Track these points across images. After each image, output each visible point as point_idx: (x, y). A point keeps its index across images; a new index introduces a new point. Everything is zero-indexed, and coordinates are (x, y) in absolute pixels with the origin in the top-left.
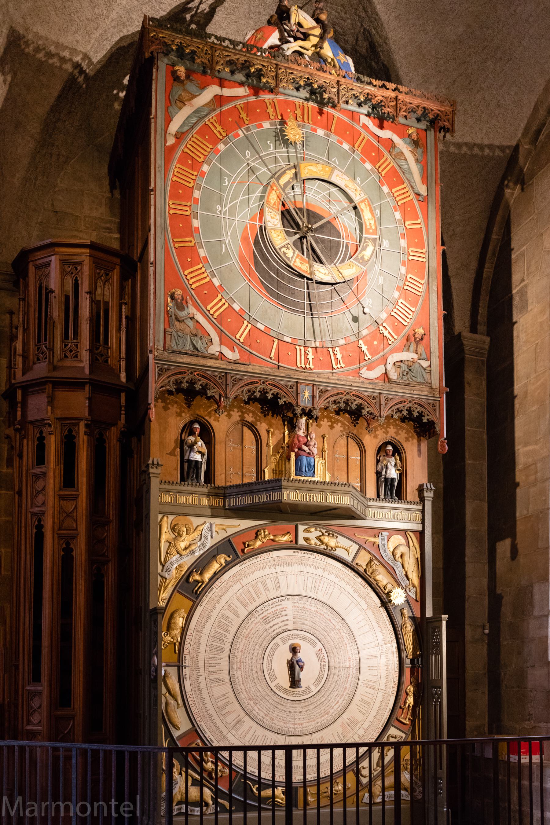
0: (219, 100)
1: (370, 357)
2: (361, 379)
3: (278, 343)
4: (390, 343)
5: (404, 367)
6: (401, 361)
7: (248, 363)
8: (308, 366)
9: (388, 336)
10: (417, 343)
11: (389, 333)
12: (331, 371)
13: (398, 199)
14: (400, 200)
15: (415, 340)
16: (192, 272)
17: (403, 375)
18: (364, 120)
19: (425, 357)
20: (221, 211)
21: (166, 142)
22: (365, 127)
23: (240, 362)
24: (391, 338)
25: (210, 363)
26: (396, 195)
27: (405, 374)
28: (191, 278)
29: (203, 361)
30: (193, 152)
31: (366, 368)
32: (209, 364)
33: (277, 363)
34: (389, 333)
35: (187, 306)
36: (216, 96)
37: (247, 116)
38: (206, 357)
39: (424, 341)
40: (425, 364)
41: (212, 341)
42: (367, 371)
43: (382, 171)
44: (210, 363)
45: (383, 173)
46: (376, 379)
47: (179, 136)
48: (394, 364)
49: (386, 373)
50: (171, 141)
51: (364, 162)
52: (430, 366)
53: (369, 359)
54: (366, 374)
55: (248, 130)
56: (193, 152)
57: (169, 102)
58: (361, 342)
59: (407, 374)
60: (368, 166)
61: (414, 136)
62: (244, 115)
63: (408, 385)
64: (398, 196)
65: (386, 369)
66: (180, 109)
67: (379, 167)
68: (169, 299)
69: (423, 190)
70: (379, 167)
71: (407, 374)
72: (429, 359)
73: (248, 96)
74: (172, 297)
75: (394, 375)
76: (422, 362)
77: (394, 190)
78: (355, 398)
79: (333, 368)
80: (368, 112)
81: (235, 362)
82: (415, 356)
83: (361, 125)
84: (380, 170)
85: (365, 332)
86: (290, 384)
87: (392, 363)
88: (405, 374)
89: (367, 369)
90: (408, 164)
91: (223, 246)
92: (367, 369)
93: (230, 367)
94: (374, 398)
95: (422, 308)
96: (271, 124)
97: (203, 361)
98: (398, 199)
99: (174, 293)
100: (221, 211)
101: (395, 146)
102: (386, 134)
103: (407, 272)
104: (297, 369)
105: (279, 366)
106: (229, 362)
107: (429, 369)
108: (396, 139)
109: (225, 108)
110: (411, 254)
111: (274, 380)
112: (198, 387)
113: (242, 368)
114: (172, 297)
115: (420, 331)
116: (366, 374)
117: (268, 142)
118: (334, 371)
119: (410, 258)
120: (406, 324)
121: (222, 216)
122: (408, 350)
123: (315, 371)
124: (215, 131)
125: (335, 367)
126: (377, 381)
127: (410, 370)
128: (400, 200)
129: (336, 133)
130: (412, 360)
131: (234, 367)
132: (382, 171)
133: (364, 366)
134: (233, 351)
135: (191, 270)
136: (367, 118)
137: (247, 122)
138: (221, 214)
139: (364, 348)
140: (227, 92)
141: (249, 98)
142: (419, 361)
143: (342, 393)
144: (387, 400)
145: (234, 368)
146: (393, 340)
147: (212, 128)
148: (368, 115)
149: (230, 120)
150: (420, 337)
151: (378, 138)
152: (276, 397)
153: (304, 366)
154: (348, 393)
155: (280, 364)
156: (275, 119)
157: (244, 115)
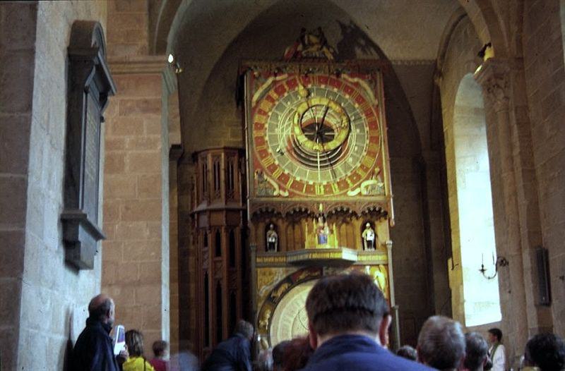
0: (274, 82)
5: (370, 188)
22: (344, 79)
25: (274, 199)
29: (271, 199)
40: (381, 185)
44: (274, 199)
47: (258, 102)
50: (254, 105)
54: (351, 193)
57: (251, 90)
62: (286, 87)
69: (376, 102)
72: (383, 181)
75: (364, 192)
76: (379, 184)
82: (376, 182)
97: (271, 199)
102: (356, 80)
112: (270, 210)
113: (290, 199)
115: (377, 170)
116: (351, 193)
139: (349, 181)
140: (278, 78)
151: (352, 83)
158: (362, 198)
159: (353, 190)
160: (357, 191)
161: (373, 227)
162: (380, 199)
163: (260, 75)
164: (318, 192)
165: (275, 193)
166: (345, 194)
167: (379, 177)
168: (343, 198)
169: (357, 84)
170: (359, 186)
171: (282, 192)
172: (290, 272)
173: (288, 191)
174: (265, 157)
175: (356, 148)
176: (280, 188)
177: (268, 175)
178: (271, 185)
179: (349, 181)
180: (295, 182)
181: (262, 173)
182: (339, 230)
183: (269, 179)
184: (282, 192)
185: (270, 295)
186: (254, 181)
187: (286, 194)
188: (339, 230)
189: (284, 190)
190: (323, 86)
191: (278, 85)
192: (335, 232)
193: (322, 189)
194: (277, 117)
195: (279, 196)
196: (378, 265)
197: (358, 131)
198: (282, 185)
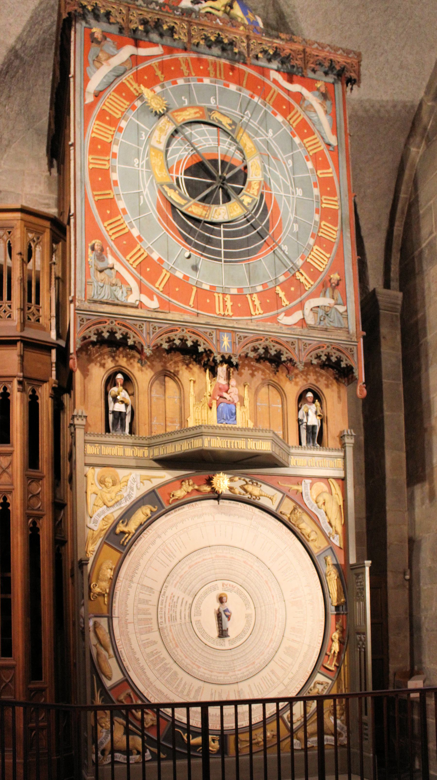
1: (287, 303)
2: (280, 325)
3: (197, 291)
4: (307, 289)
5: (321, 312)
6: (318, 307)
7: (168, 311)
8: (226, 313)
9: (305, 282)
10: (334, 288)
11: (305, 279)
12: (249, 318)
13: (309, 149)
14: (311, 150)
15: (331, 285)
16: (111, 224)
17: (321, 320)
18: (274, 75)
19: (342, 302)
20: (138, 165)
21: (85, 100)
22: (275, 82)
23: (159, 310)
24: (307, 284)
26: (307, 145)
27: (322, 319)
28: (111, 229)
30: (110, 109)
31: (283, 314)
32: (129, 313)
33: (196, 310)
34: (305, 279)
35: (107, 257)
36: (132, 56)
37: (162, 73)
38: (126, 306)
39: (340, 287)
40: (341, 309)
41: (131, 291)
42: (285, 318)
43: (294, 122)
45: (294, 125)
46: (295, 324)
47: (98, 95)
48: (311, 310)
49: (304, 319)
51: (276, 114)
52: (346, 311)
53: (286, 305)
55: (163, 86)
56: (110, 109)
57: (86, 64)
58: (278, 288)
59: (324, 319)
60: (280, 118)
61: (323, 89)
62: (159, 73)
63: (326, 330)
64: (309, 146)
65: (303, 315)
66: (98, 68)
67: (290, 119)
68: (90, 250)
69: (333, 140)
70: (290, 119)
71: (324, 319)
73: (162, 55)
74: (93, 249)
75: (310, 320)
76: (338, 307)
77: (305, 141)
78: (274, 344)
79: (252, 315)
80: (278, 67)
81: (155, 311)
82: (332, 302)
83: (272, 80)
84: (291, 122)
85: (282, 279)
86: (209, 331)
87: (309, 309)
88: (322, 319)
89: (285, 315)
90: (317, 116)
91: (141, 197)
92: (285, 315)
93: (150, 316)
94: (293, 344)
95: (337, 254)
96: (185, 81)
98: (309, 149)
99: (94, 245)
100: (138, 165)
101: (305, 99)
102: (295, 88)
103: (321, 219)
104: (216, 316)
105: (198, 313)
106: (149, 310)
107: (345, 313)
108: (305, 92)
109: (141, 67)
110: (324, 201)
111: (193, 327)
112: (118, 336)
113: (161, 316)
114: (93, 249)
115: (335, 277)
117: (183, 98)
118: (253, 317)
119: (324, 206)
120: (321, 270)
121: (140, 168)
122: (324, 295)
123: (234, 318)
124: (132, 89)
125: (253, 313)
126: (295, 327)
127: (327, 315)
128: (311, 150)
129: (248, 87)
130: (328, 305)
131: (154, 315)
132: (294, 122)
133: (282, 312)
134: (152, 299)
135: (110, 221)
136: (277, 73)
137: (162, 79)
138: (139, 167)
139: (282, 294)
140: (142, 52)
141: (164, 56)
142: (336, 306)
143: (261, 340)
144: (305, 345)
145: (154, 316)
146: (310, 286)
147: (129, 86)
148: (278, 70)
149: (146, 77)
150: (336, 282)
151: (288, 92)
152: (196, 344)
153: (223, 313)
154: (267, 340)
155: (199, 312)
156: (189, 75)
157: (159, 73)
158: (305, 331)
159: (288, 313)
160: (297, 316)
161: (317, 397)
162: (343, 336)
163: (105, 38)
164: (219, 310)
165: (132, 299)
166: (274, 319)
167: (337, 294)
168: (269, 326)
169: (299, 97)
170: (301, 306)
171: (145, 299)
172: (156, 482)
173: (158, 297)
174: (110, 217)
175: (296, 228)
176: (142, 289)
177: (114, 255)
178: (124, 281)
179: (282, 294)
180: (173, 278)
181: (102, 250)
182: (256, 401)
183: (118, 267)
184: (145, 299)
185: (115, 527)
186: (87, 263)
187: (154, 304)
188: (256, 401)
189: (150, 295)
190: (233, 87)
191: (141, 67)
192: (246, 403)
193: (229, 304)
194: (139, 134)
195: (140, 305)
196: (327, 478)
197: (299, 192)
198: (145, 282)
